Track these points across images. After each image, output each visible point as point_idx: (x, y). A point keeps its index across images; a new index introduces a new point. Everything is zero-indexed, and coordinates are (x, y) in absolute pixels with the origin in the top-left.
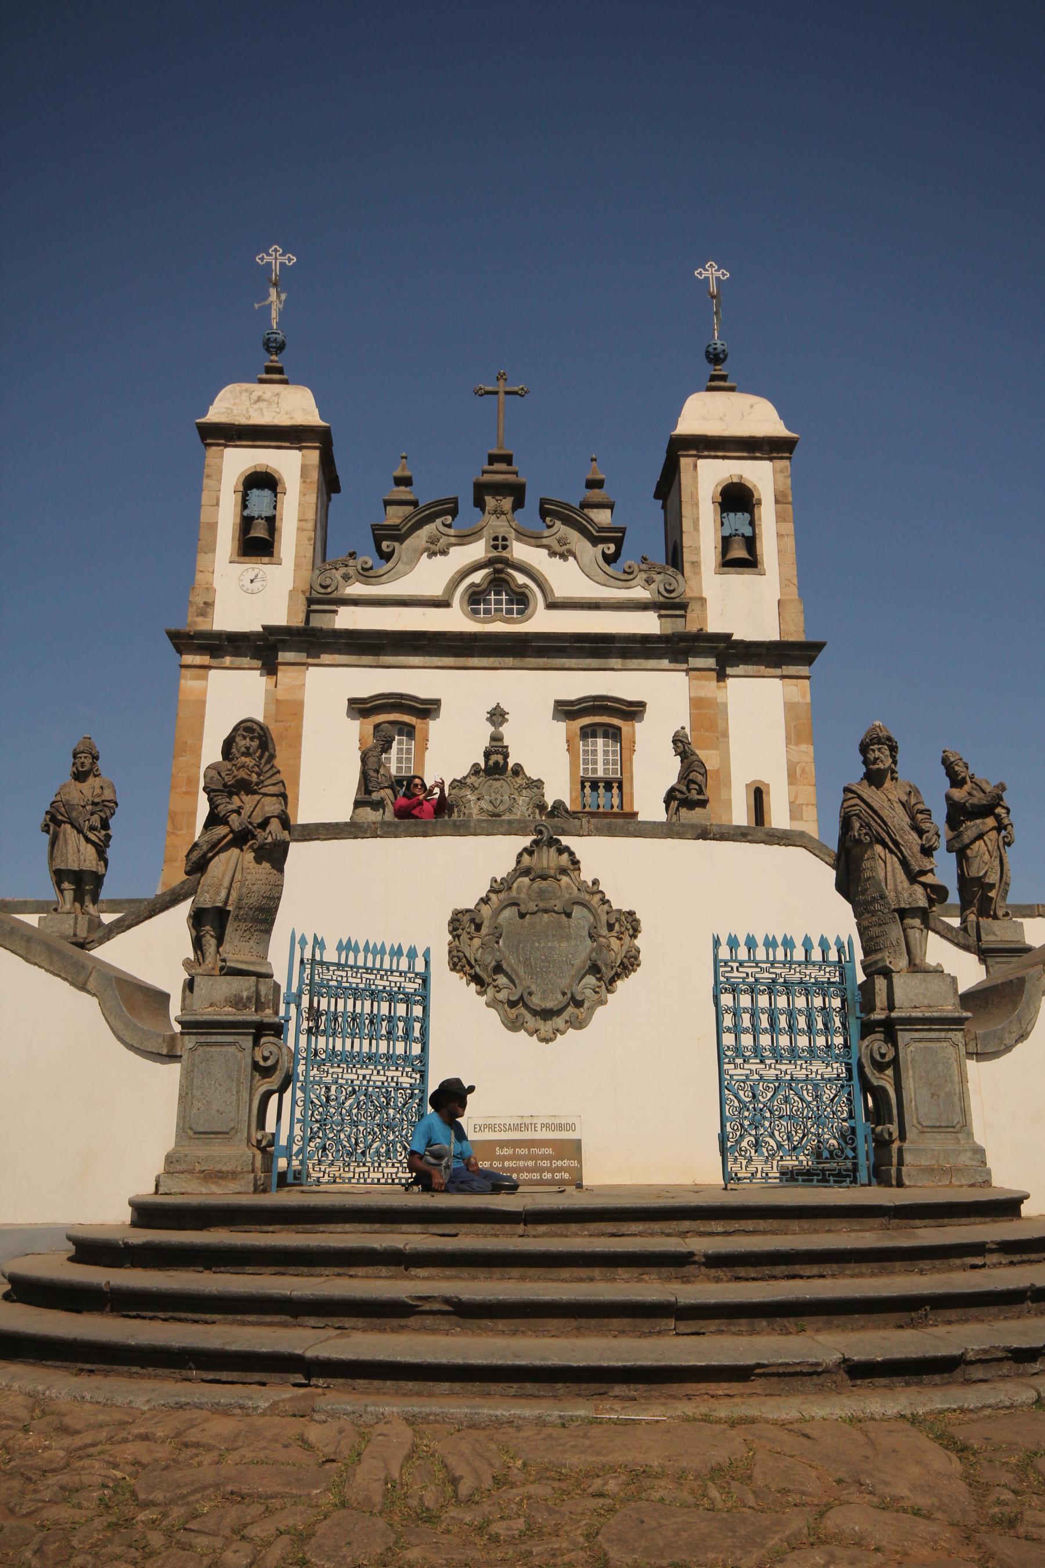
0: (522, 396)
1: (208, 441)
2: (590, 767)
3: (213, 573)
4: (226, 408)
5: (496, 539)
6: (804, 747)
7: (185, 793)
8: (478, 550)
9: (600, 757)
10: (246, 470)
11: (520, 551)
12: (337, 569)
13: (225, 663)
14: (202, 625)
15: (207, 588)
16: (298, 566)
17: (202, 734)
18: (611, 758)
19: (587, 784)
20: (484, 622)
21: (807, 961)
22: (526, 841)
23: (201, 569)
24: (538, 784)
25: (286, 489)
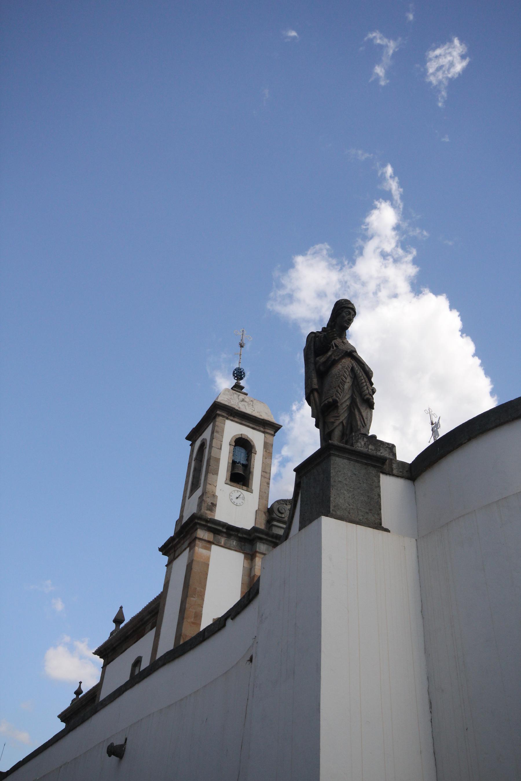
1: (218, 412)
3: (216, 487)
4: (227, 399)
7: (194, 623)
10: (236, 435)
12: (286, 504)
13: (221, 543)
14: (209, 515)
15: (213, 495)
16: (261, 497)
17: (205, 585)
23: (210, 483)
25: (256, 451)
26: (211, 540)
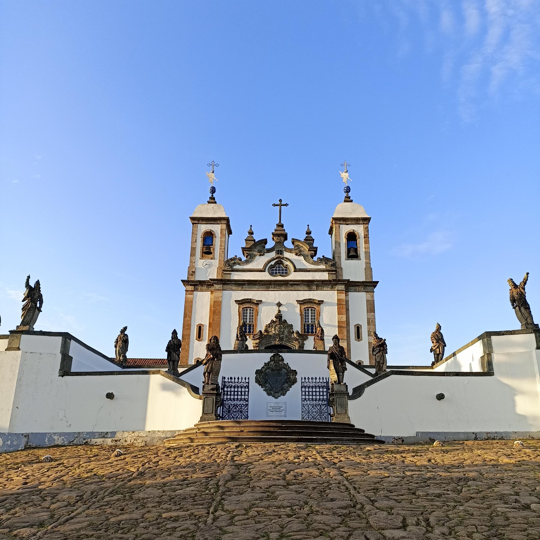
0: (287, 206)
2: (307, 320)
5: (278, 251)
6: (372, 314)
7: (187, 329)
8: (273, 254)
9: (310, 317)
11: (286, 255)
18: (313, 317)
19: (306, 326)
20: (274, 276)
21: (320, 382)
22: (272, 354)
24: (291, 326)
26: (193, 290)
